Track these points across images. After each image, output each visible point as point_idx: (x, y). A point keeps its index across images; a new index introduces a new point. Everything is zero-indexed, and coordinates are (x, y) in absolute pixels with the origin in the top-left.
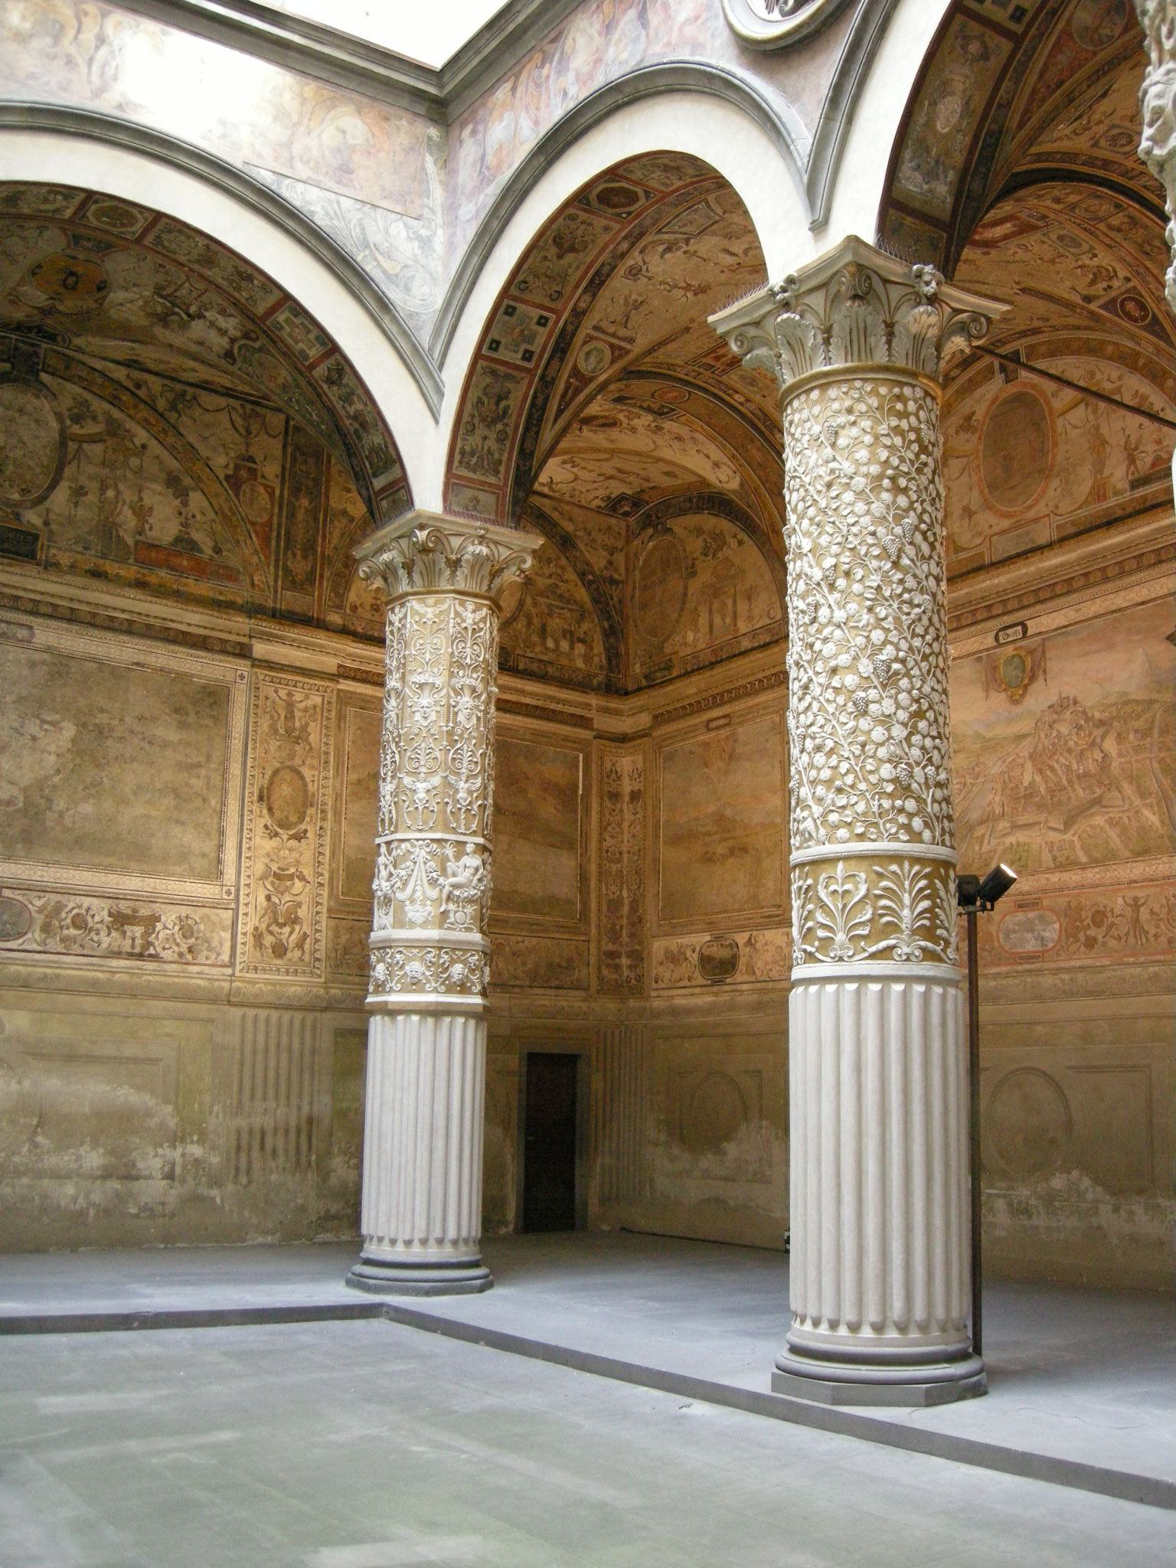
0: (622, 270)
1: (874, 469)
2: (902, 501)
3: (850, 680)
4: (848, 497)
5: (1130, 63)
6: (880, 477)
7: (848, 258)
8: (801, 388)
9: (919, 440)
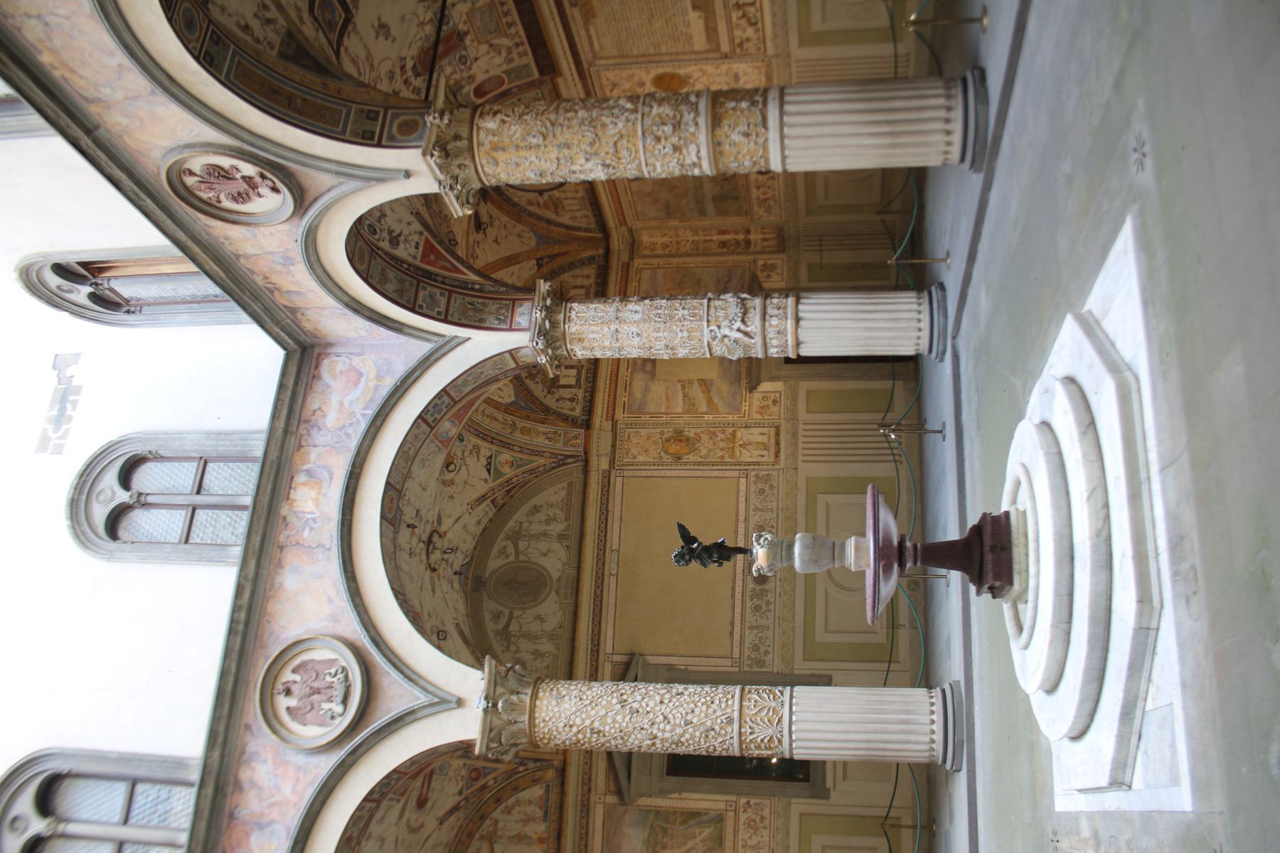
3: (668, 696)
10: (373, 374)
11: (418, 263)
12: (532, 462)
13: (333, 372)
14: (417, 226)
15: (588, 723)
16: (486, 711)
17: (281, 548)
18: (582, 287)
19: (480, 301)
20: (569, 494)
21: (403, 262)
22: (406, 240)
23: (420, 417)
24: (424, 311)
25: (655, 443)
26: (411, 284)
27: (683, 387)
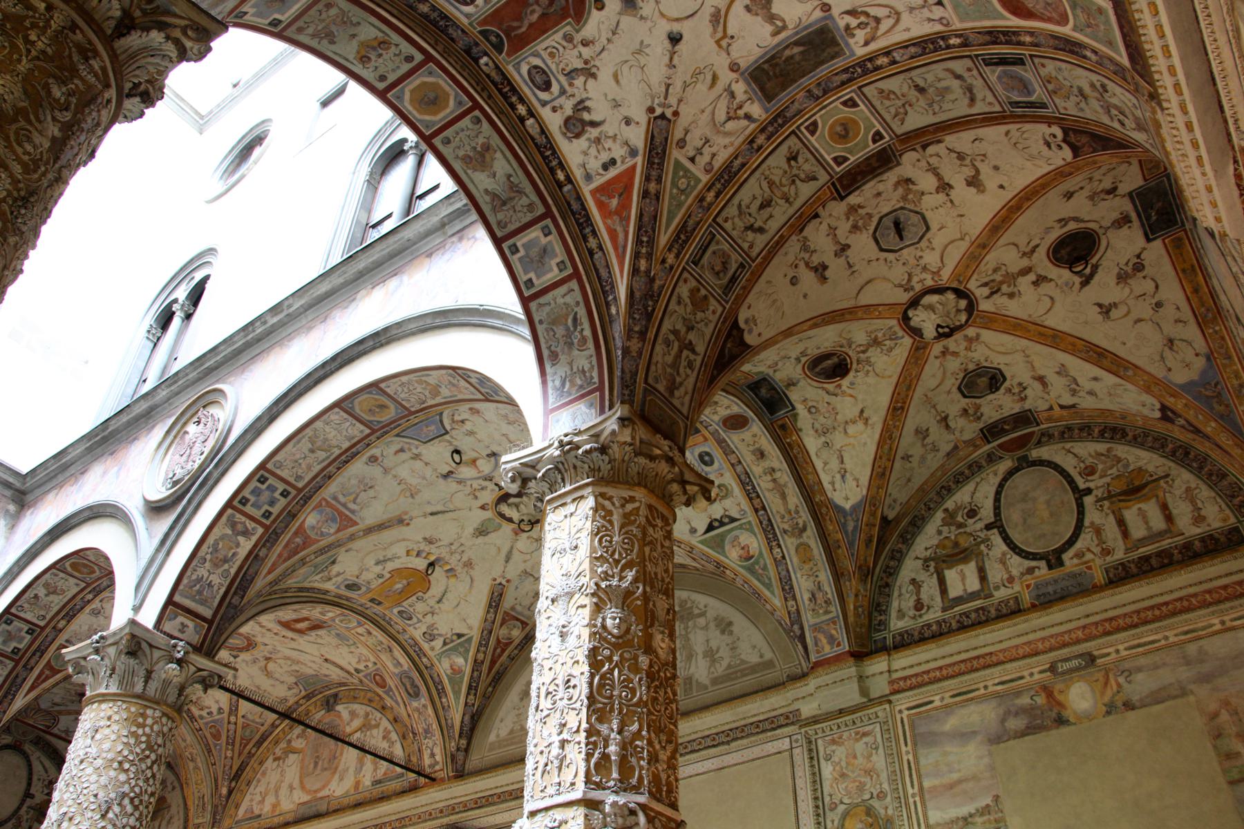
0: (87, 609)
1: (110, 756)
2: (123, 777)
4: (89, 770)
5: (343, 549)
6: (112, 760)
7: (127, 631)
8: (92, 701)
9: (148, 742)
11: (586, 190)
12: (768, 586)
14: (637, 136)
18: (1169, 518)
19: (588, 333)
20: (754, 669)
21: (561, 166)
22: (598, 141)
24: (514, 259)
25: (861, 787)
26: (531, 207)
27: (986, 810)
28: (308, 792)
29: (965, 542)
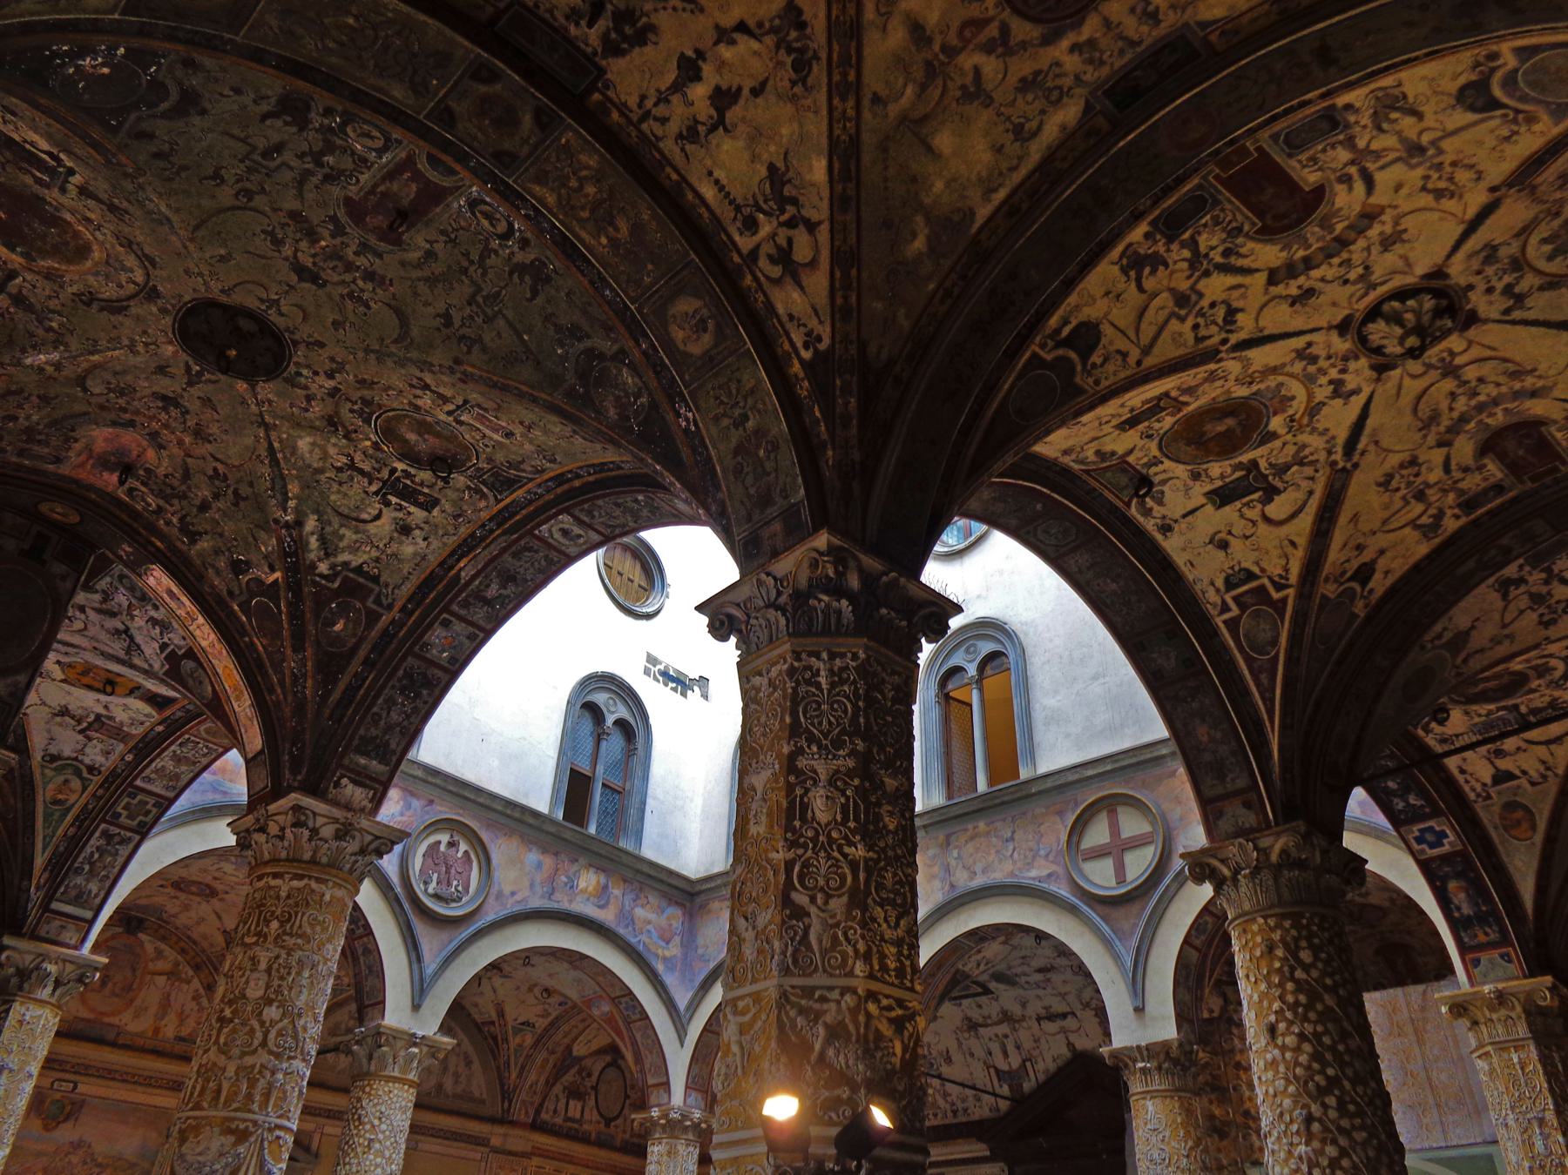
10: (667, 953)
13: (674, 917)
15: (381, 1136)
16: (414, 1035)
17: (556, 854)
23: (631, 993)
28: (93, 1010)
29: (582, 1089)
